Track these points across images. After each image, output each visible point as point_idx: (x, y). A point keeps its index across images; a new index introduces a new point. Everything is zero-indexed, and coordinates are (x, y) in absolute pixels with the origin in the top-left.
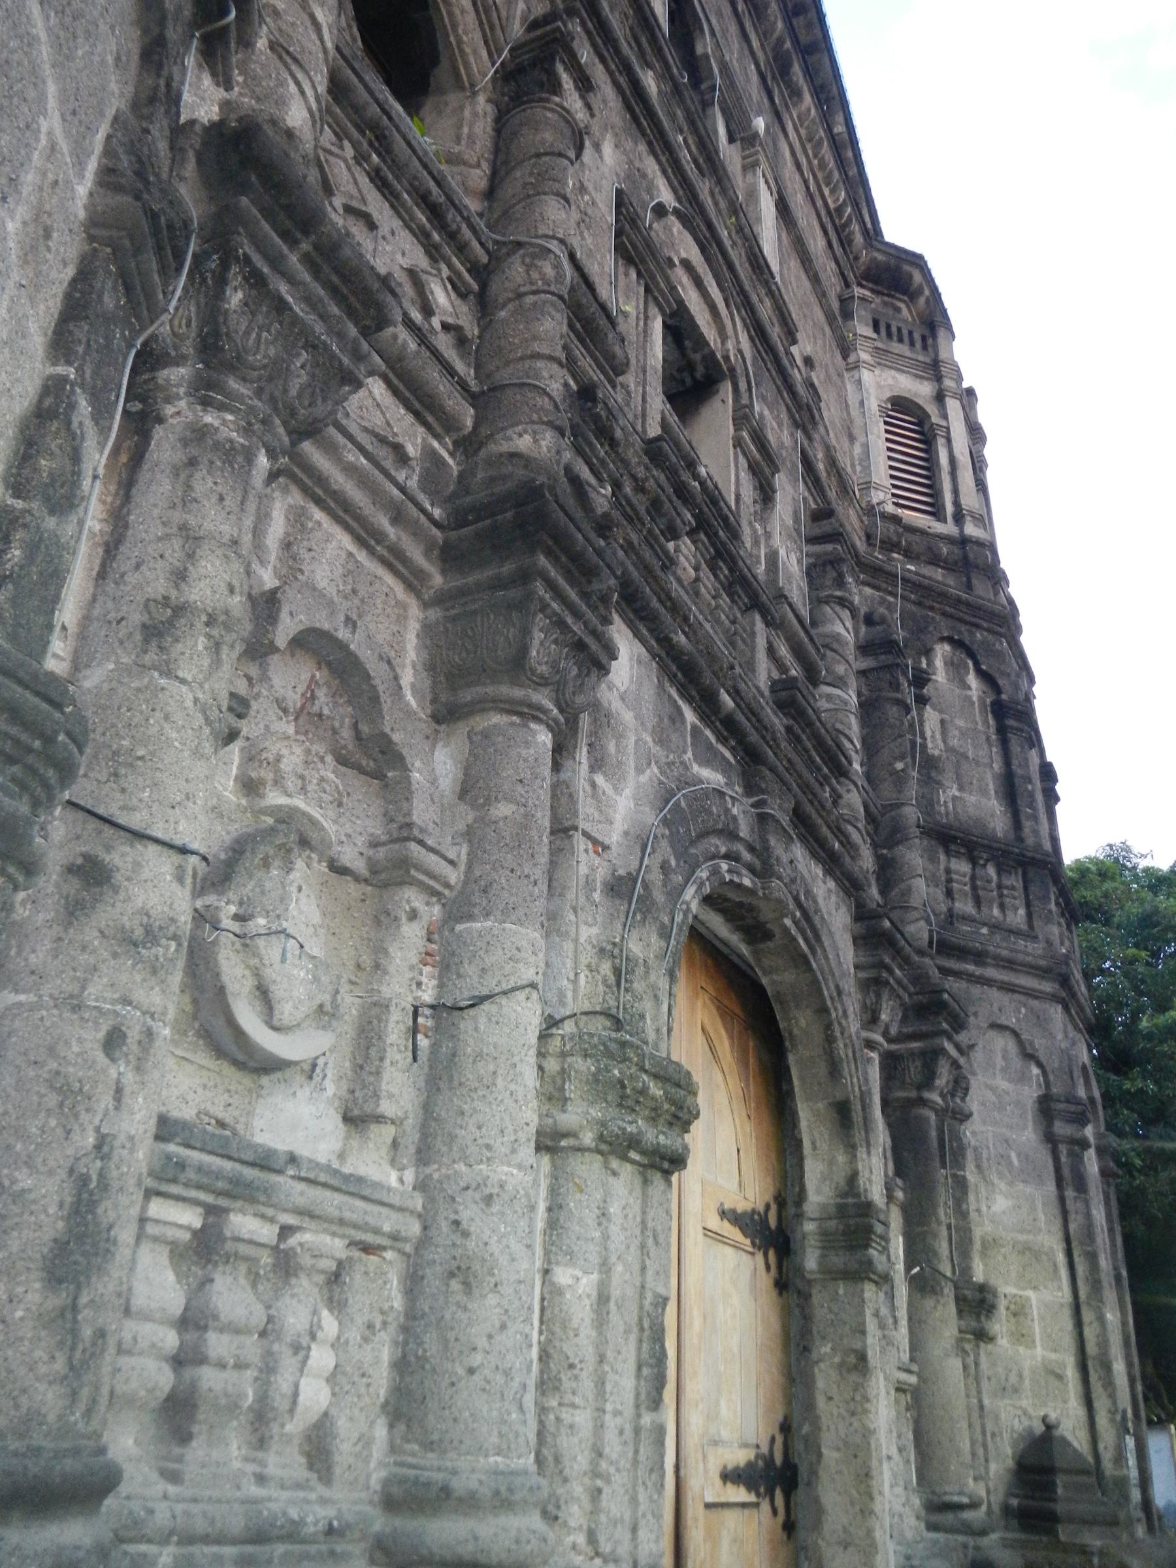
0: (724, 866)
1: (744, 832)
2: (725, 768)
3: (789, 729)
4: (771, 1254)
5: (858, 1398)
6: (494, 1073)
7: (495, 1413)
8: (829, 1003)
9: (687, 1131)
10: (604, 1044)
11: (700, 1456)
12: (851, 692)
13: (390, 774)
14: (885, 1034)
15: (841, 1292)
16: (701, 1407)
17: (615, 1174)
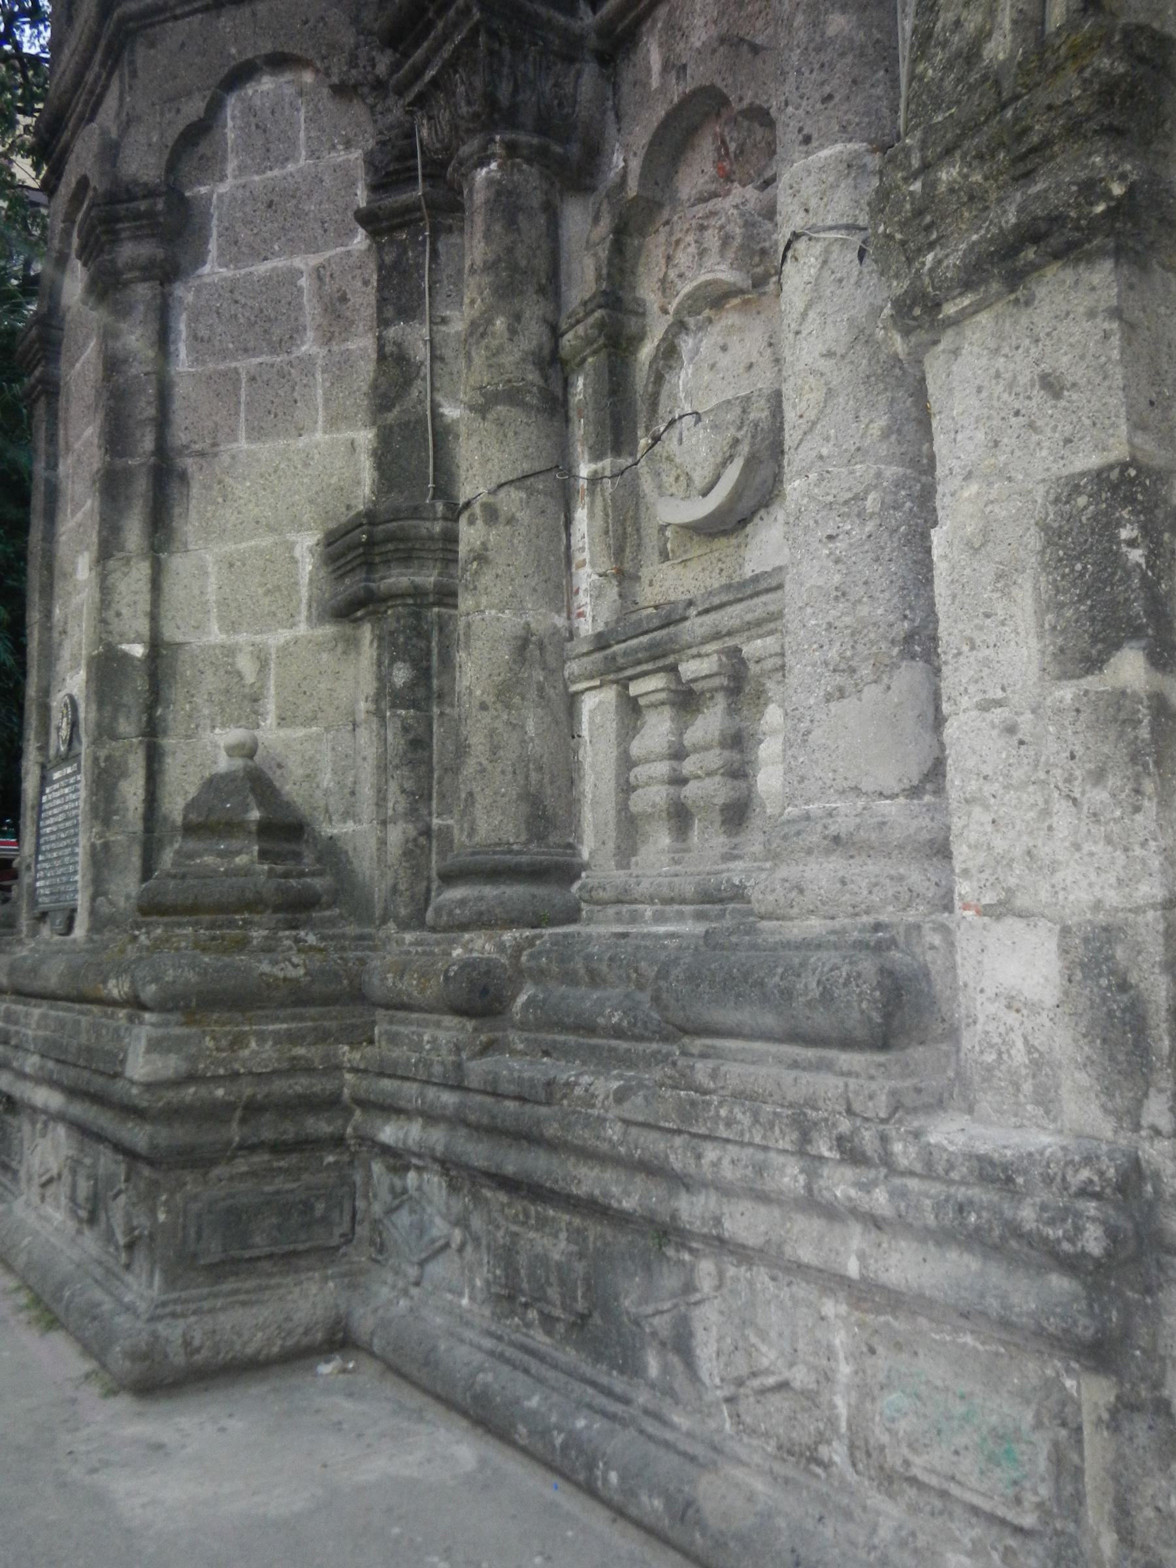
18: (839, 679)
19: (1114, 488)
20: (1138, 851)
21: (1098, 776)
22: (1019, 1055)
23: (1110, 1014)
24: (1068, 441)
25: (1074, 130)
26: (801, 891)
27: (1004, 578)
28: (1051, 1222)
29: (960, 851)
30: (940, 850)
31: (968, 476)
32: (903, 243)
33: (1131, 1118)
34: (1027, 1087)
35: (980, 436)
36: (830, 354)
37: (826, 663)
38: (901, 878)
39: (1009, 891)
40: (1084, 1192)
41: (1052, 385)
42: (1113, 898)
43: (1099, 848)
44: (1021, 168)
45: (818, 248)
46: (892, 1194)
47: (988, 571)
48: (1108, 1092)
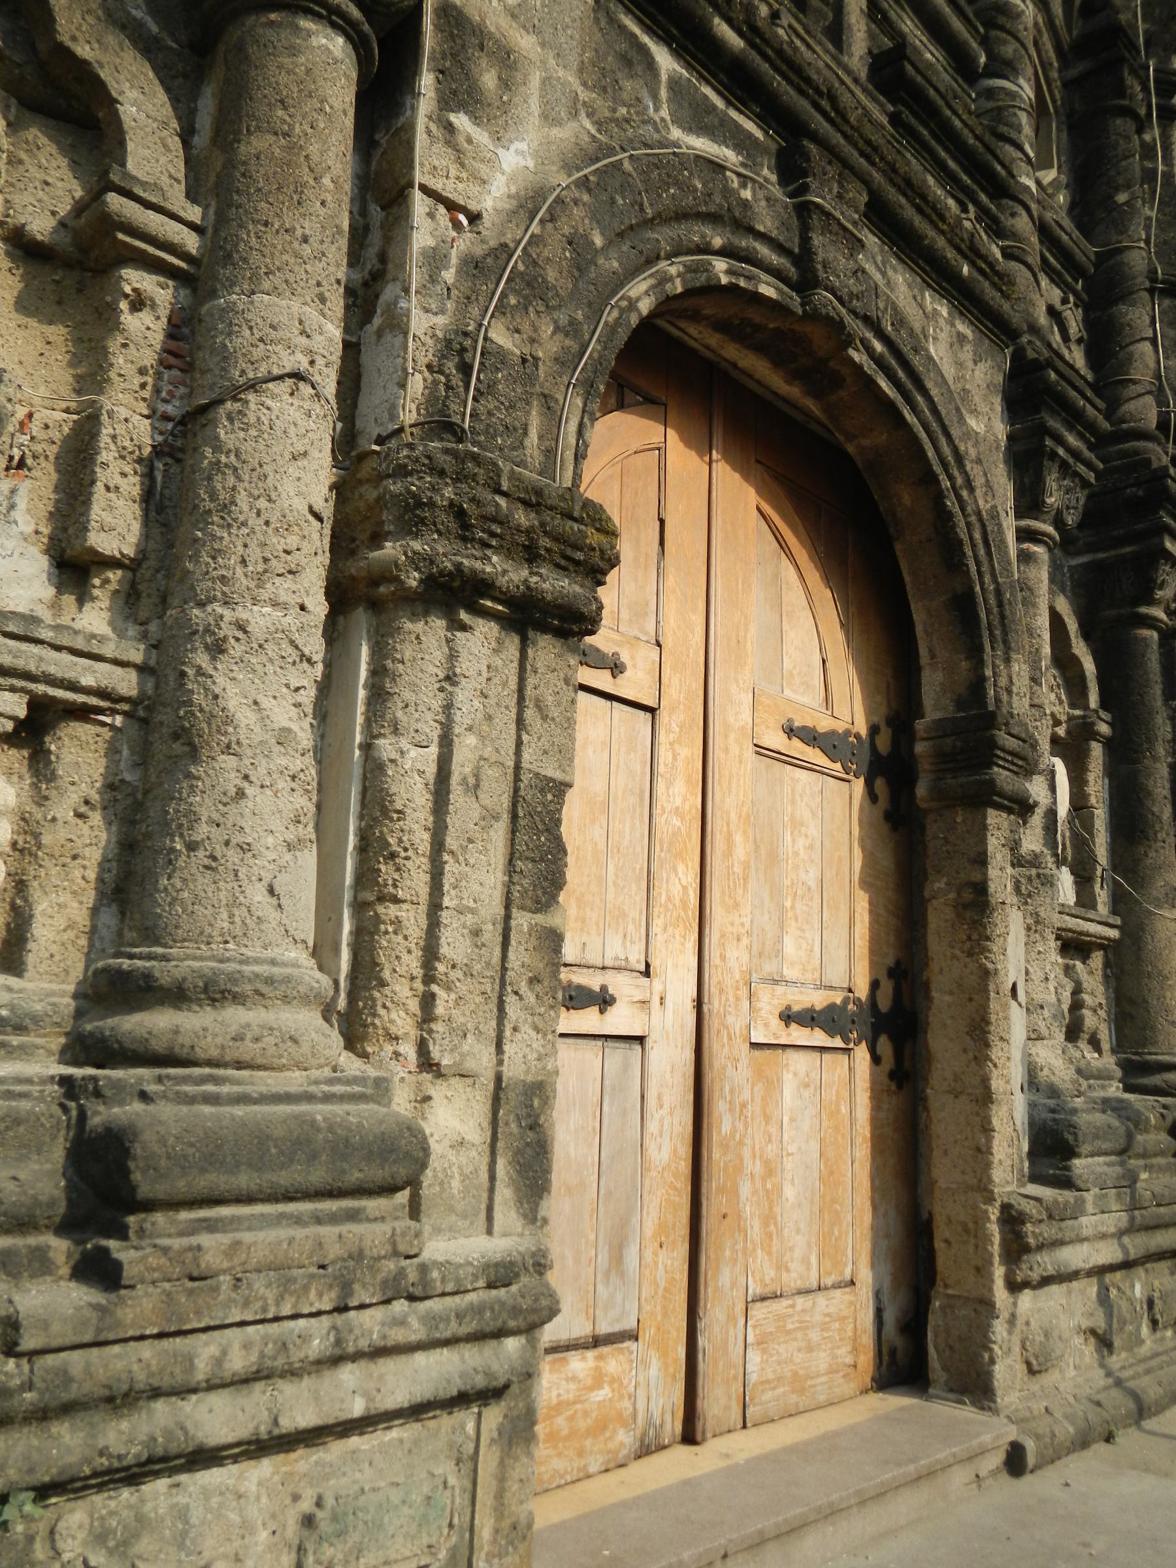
0: (720, 265)
1: (766, 223)
2: (740, 141)
3: (895, 119)
4: (880, 784)
5: (975, 937)
6: (234, 489)
7: (222, 895)
8: (937, 468)
9: (601, 583)
10: (429, 457)
11: (743, 993)
12: (1022, 81)
13: (100, 115)
14: (1058, 523)
15: (959, 820)
16: (745, 941)
17: (464, 628)
39: (462, 1055)
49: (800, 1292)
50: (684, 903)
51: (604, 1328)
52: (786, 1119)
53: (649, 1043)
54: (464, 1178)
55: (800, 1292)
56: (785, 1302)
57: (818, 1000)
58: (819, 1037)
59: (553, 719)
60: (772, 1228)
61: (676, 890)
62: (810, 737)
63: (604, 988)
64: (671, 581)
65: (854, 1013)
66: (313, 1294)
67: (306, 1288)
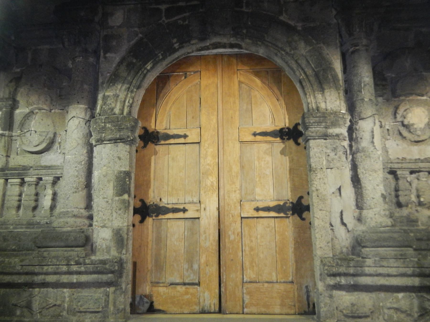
11: (239, 205)
18: (75, 190)
19: (126, 174)
20: (125, 219)
21: (120, 209)
22: (104, 246)
23: (119, 240)
24: (121, 166)
25: (127, 128)
26: (67, 223)
27: (109, 181)
28: (111, 267)
29: (95, 219)
30: (91, 218)
31: (105, 166)
32: (99, 131)
33: (121, 253)
34: (105, 251)
35: (107, 161)
36: (79, 138)
37: (73, 187)
38: (84, 222)
39: (105, 224)
40: (116, 262)
41: (119, 158)
42: (121, 225)
43: (119, 219)
44: (119, 130)
45: (78, 121)
46: (85, 268)
47: (106, 180)
48: (118, 250)
49: (267, 282)
50: (212, 186)
51: (187, 281)
52: (259, 236)
53: (200, 219)
54: (106, 245)
55: (267, 282)
56: (259, 284)
57: (272, 204)
58: (273, 214)
59: (122, 159)
60: (254, 264)
61: (209, 183)
62: (264, 134)
63: (184, 208)
64: (203, 111)
65: (289, 206)
66: (62, 261)
67: (61, 261)
